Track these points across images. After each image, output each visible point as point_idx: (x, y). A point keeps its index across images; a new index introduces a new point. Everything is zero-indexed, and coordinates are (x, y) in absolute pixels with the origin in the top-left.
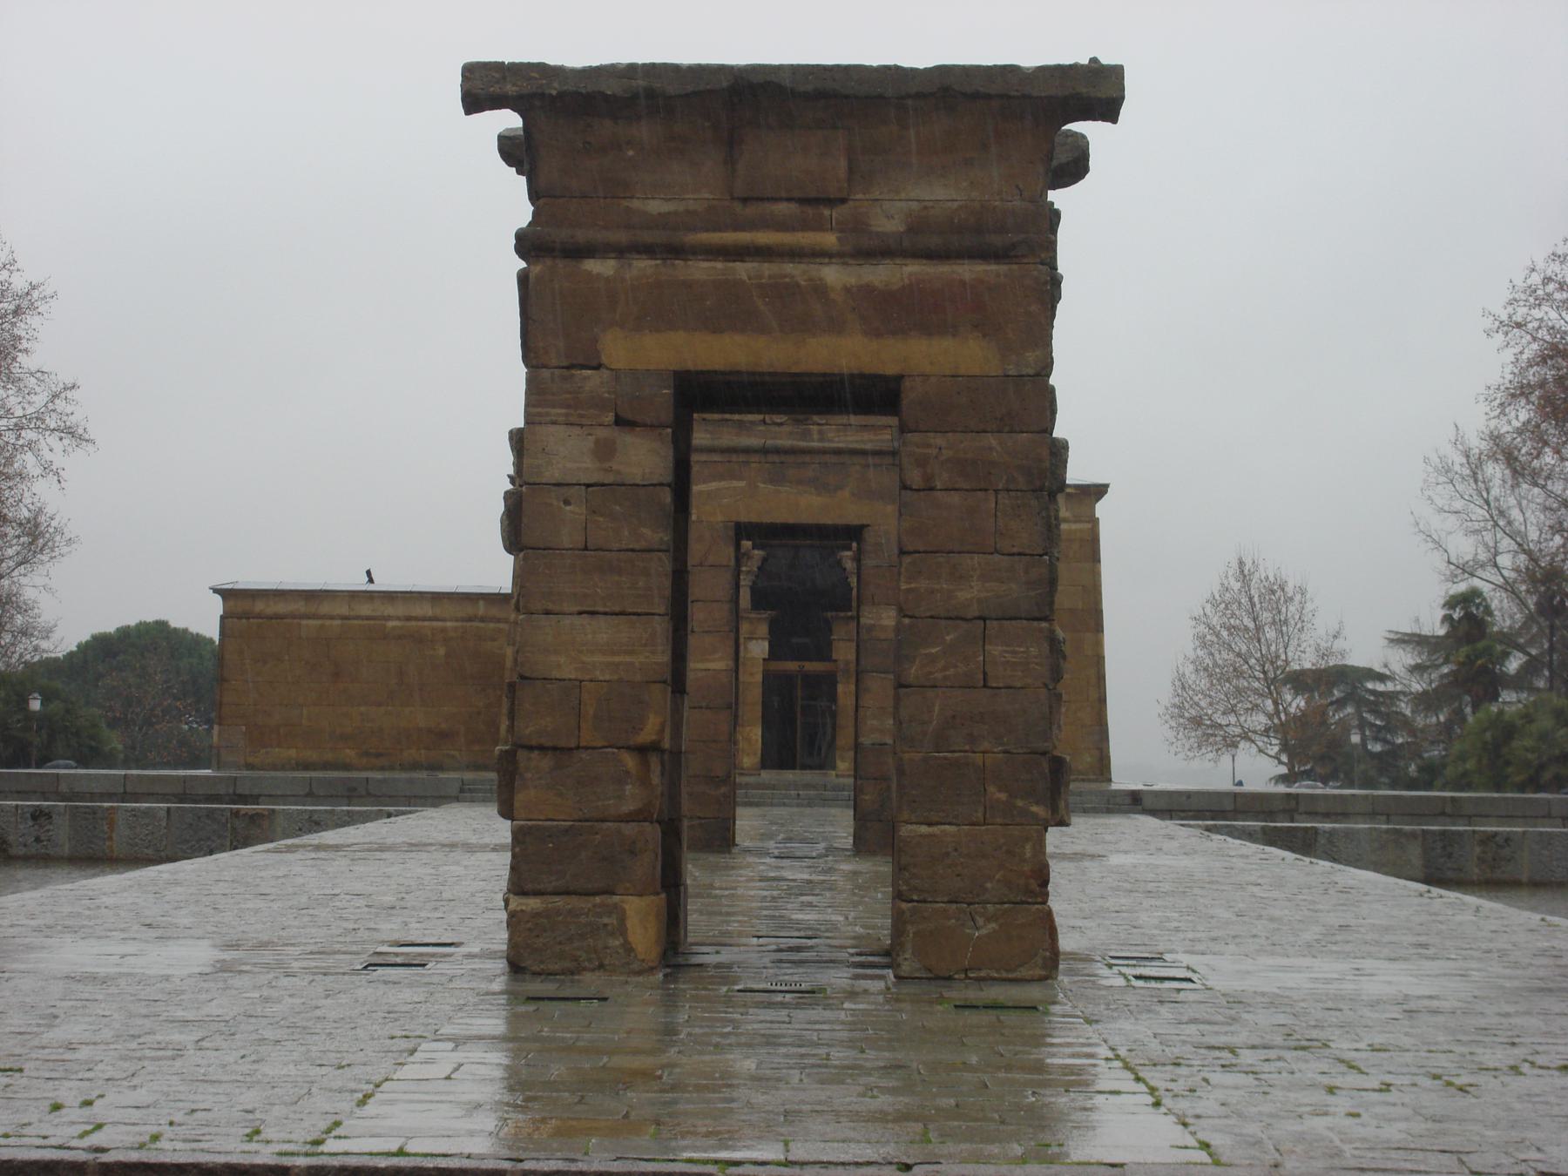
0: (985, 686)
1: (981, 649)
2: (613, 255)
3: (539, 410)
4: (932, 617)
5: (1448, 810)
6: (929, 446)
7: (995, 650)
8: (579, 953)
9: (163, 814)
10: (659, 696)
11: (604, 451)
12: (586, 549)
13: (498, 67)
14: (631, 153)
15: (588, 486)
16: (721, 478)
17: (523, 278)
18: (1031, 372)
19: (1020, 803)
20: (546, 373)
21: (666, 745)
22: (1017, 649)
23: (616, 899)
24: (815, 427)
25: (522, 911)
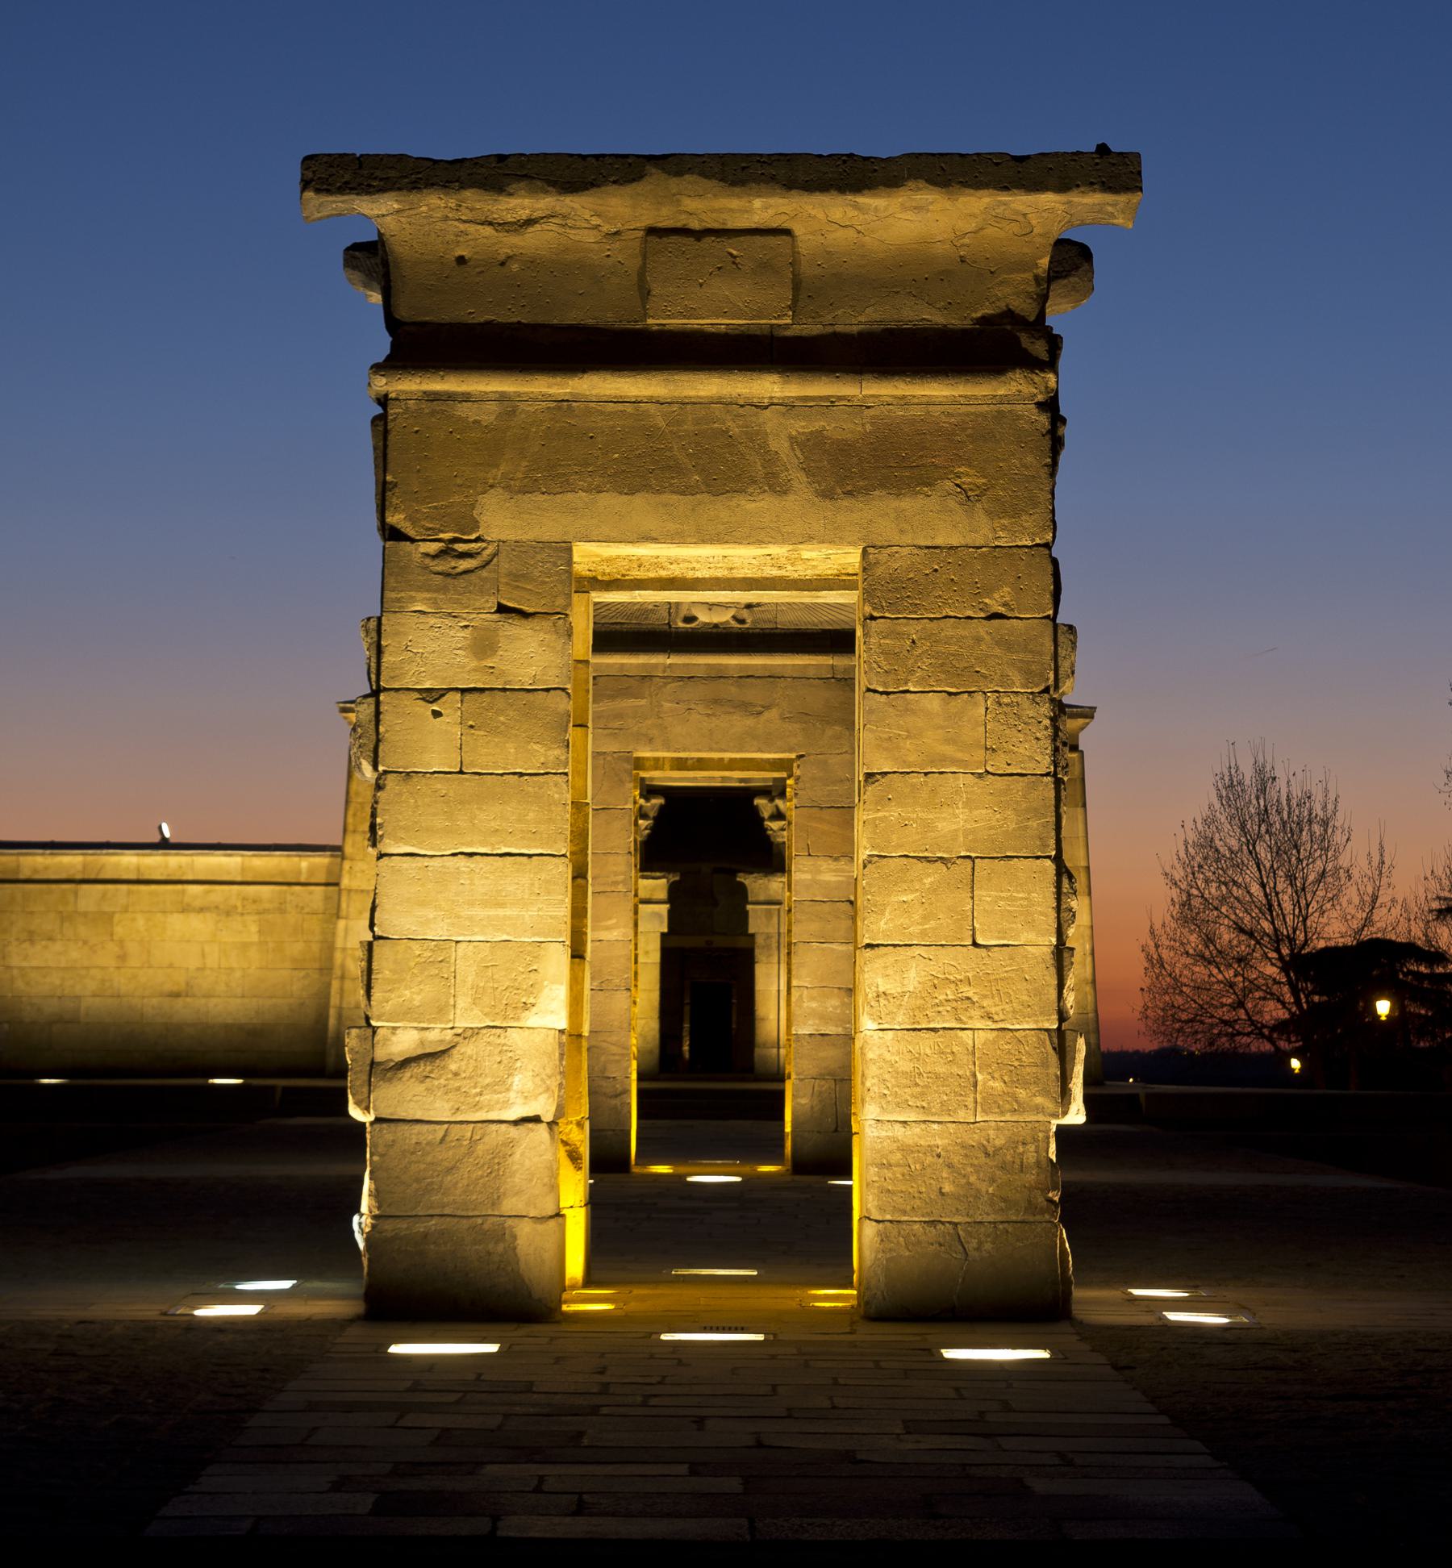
6: (899, 635)
10: (558, 958)
11: (483, 646)
12: (461, 772)
15: (463, 691)
16: (612, 697)
19: (1022, 1094)
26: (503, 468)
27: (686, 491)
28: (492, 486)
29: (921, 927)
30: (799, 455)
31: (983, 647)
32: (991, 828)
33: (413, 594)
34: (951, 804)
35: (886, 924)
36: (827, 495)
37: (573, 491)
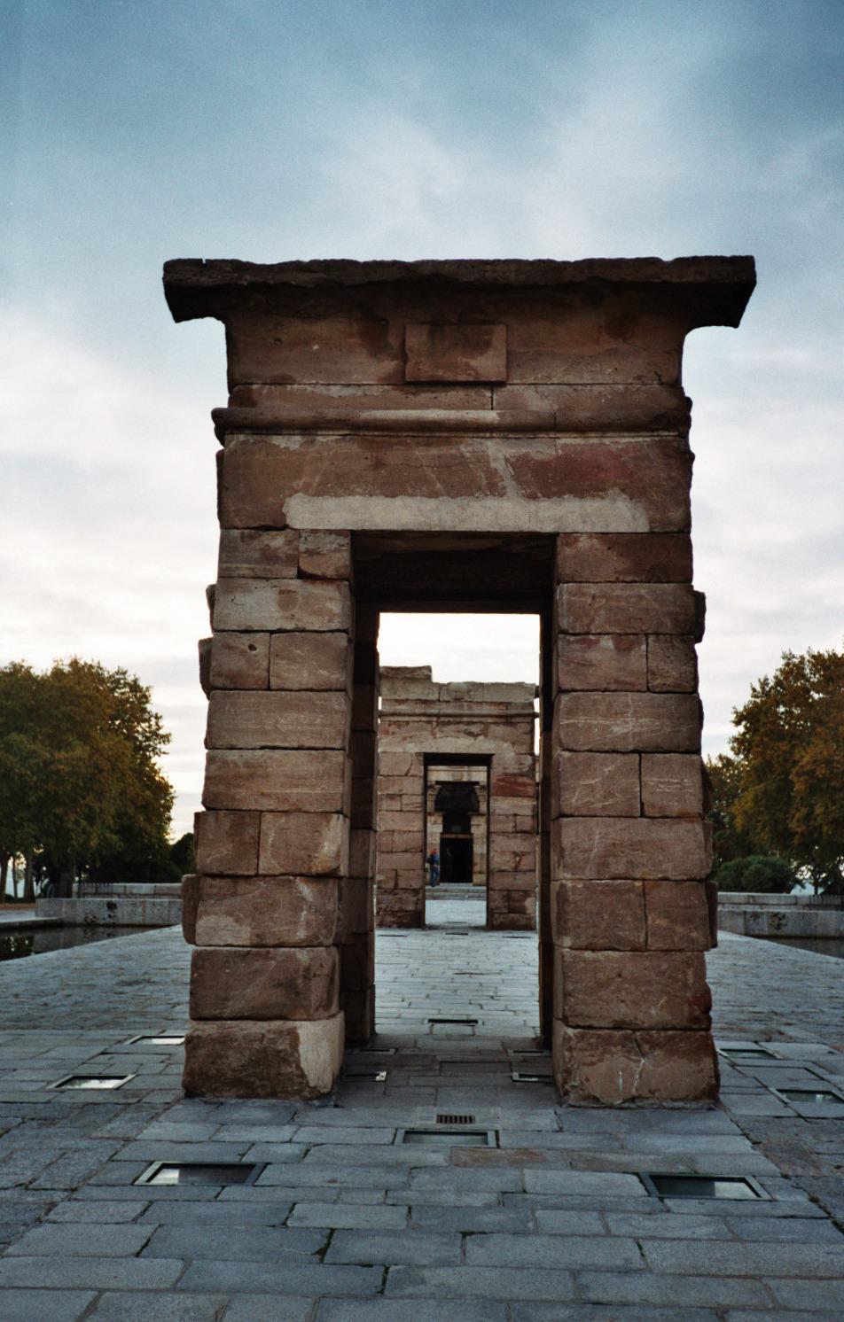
0: (643, 815)
1: (638, 781)
2: (297, 432)
3: (229, 565)
4: (590, 751)
5: (751, 901)
6: (584, 595)
7: (651, 780)
8: (252, 1079)
9: (167, 904)
11: (287, 600)
13: (197, 263)
14: (316, 347)
15: (272, 632)
17: (220, 457)
18: (675, 530)
19: (679, 929)
20: (236, 533)
21: (343, 871)
22: (671, 780)
23: (290, 1024)
24: (465, 704)
25: (199, 1037)
26: (304, 479)
27: (433, 494)
28: (296, 491)
29: (601, 804)
30: (511, 470)
31: (644, 602)
32: (652, 731)
33: (239, 565)
34: (623, 714)
35: (577, 801)
36: (532, 497)
37: (352, 493)
